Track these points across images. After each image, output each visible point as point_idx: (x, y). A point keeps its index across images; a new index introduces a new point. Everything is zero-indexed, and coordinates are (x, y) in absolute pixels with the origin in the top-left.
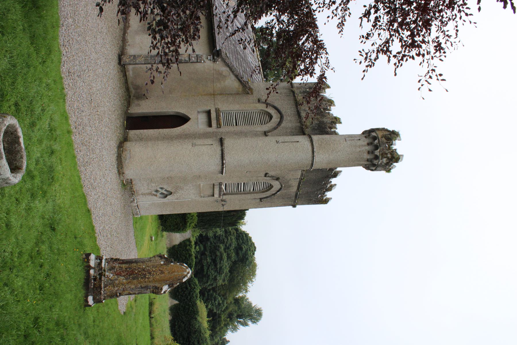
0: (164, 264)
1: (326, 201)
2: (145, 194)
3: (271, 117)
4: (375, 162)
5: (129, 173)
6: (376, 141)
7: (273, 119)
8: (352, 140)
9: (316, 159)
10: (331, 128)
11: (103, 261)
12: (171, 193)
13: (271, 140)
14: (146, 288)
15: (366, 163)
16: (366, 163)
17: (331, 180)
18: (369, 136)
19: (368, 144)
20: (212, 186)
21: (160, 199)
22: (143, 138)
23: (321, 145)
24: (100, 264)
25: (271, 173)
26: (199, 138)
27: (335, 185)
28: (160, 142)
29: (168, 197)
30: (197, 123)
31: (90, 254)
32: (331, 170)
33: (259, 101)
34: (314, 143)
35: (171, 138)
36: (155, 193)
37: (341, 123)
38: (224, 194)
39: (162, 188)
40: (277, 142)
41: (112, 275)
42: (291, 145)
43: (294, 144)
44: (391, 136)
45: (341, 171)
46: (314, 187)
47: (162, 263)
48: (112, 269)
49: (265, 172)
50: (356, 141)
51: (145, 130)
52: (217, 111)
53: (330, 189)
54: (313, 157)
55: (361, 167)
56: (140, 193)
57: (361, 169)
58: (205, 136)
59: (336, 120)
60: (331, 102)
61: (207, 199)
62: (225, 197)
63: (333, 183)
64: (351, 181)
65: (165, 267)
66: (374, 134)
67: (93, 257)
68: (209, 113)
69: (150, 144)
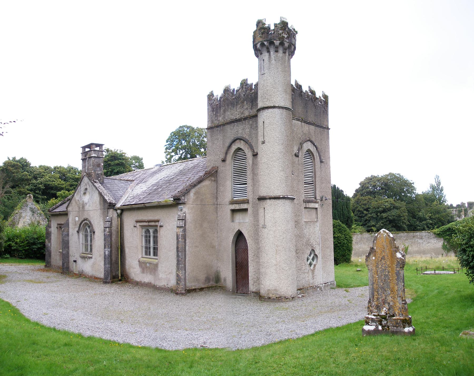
0: (375, 256)
1: (326, 97)
2: (313, 277)
3: (239, 149)
4: (286, 45)
5: (287, 289)
6: (265, 43)
7: (242, 147)
8: (264, 68)
9: (282, 104)
10: (251, 89)
11: (370, 316)
12: (313, 250)
13: (261, 149)
14: (398, 274)
15: (287, 54)
16: (287, 54)
17: (304, 91)
18: (260, 50)
19: (269, 52)
20: (306, 210)
21: (319, 262)
22: (257, 277)
23: (268, 99)
24: (373, 320)
25: (296, 151)
26: (258, 221)
27: (309, 87)
28: (261, 261)
29: (316, 253)
30: (244, 223)
31: (363, 330)
32: (293, 90)
33: (224, 161)
34: (265, 106)
35: (258, 250)
36: (312, 266)
37: (247, 80)
38: (315, 198)
39: (308, 259)
40: (263, 143)
41: (385, 309)
42: (267, 129)
43: (265, 126)
44: (262, 29)
45: (296, 81)
46: (310, 109)
47: (374, 258)
48: (378, 308)
49: (294, 157)
50: (265, 63)
51: (250, 275)
52: (233, 203)
53: (313, 92)
54: (279, 107)
55: (291, 60)
56: (311, 281)
57: (294, 61)
58: (256, 215)
59: (244, 84)
60: (226, 90)
61: (319, 216)
62: (318, 198)
63: (308, 90)
64: (305, 70)
65: (378, 255)
66: (258, 46)
67: (367, 328)
68: (233, 211)
69: (262, 270)
